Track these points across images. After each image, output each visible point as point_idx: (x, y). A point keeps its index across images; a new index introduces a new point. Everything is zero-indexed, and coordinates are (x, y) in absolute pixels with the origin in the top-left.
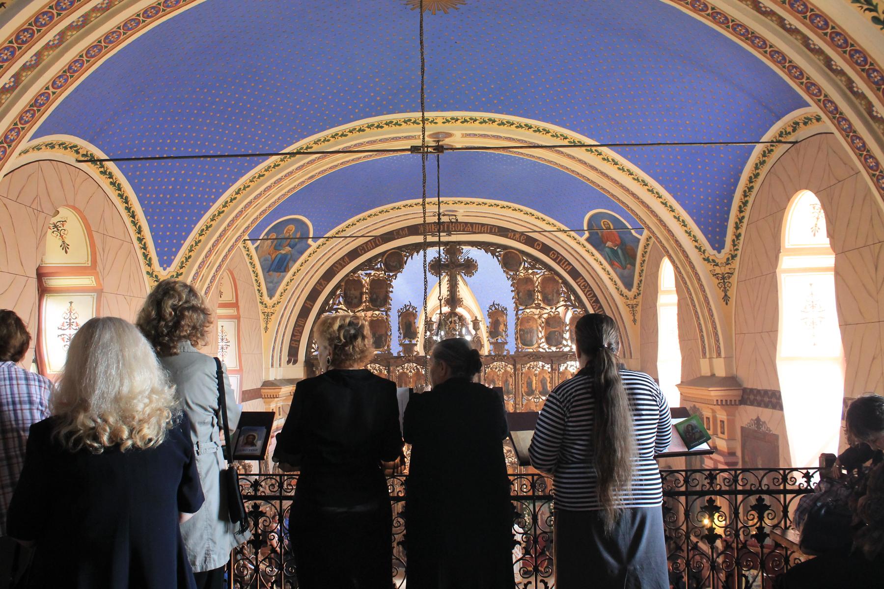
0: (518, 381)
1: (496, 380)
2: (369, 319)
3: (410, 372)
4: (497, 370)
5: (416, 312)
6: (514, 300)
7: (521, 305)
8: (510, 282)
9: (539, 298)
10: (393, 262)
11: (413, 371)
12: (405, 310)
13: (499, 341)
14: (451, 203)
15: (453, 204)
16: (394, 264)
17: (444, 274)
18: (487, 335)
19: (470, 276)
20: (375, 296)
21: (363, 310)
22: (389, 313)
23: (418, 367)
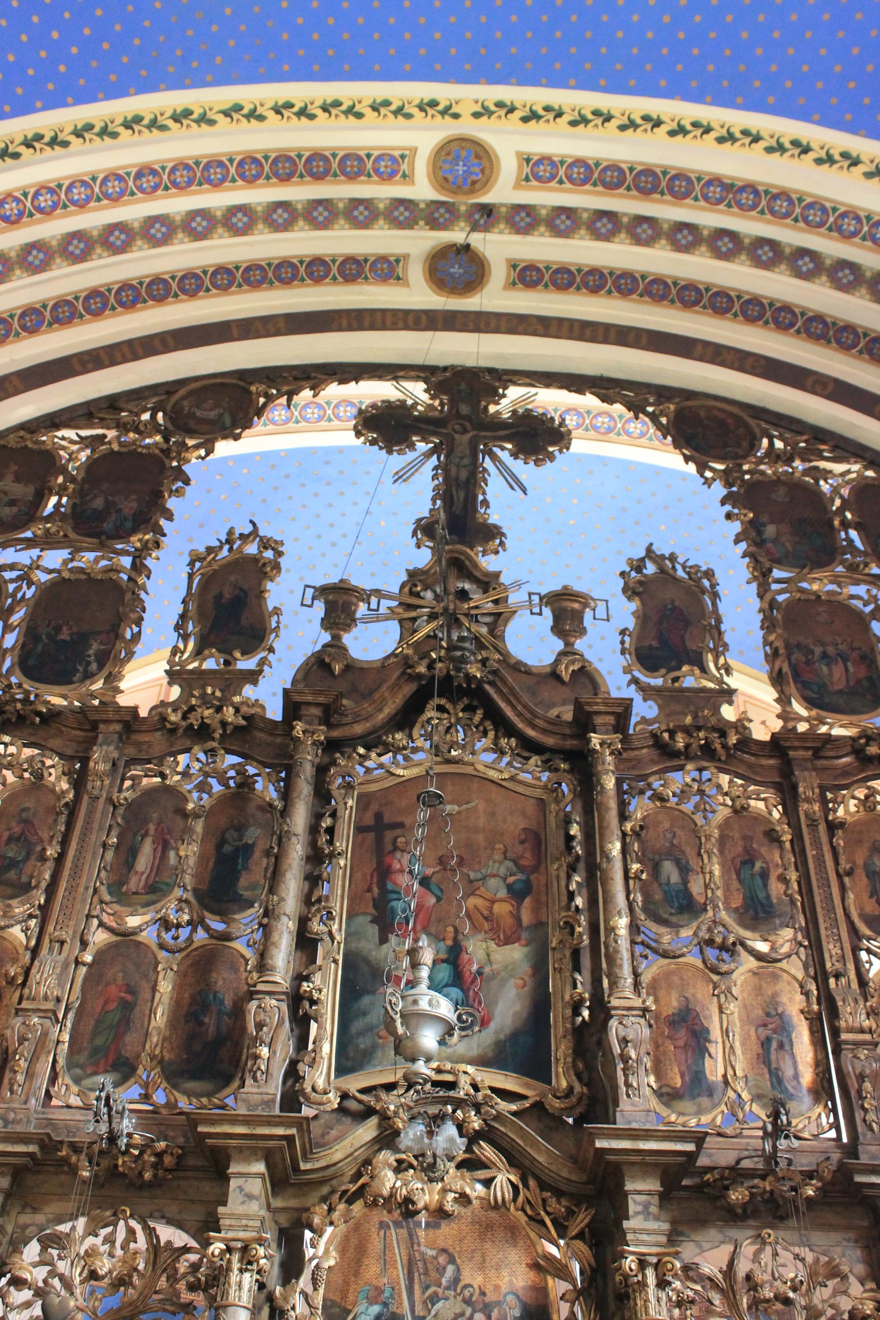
0: (820, 859)
1: (690, 853)
2: (43, 577)
3: (203, 787)
4: (688, 807)
5: (280, 554)
6: (743, 546)
7: (779, 562)
8: (719, 490)
9: (858, 544)
10: (211, 409)
11: (217, 788)
12: (225, 552)
13: (689, 682)
14: (466, 110)
15: (476, 115)
16: (212, 414)
17: (422, 447)
18: (622, 661)
19: (537, 463)
20: (98, 503)
21: (30, 543)
22: (149, 562)
23: (251, 770)
